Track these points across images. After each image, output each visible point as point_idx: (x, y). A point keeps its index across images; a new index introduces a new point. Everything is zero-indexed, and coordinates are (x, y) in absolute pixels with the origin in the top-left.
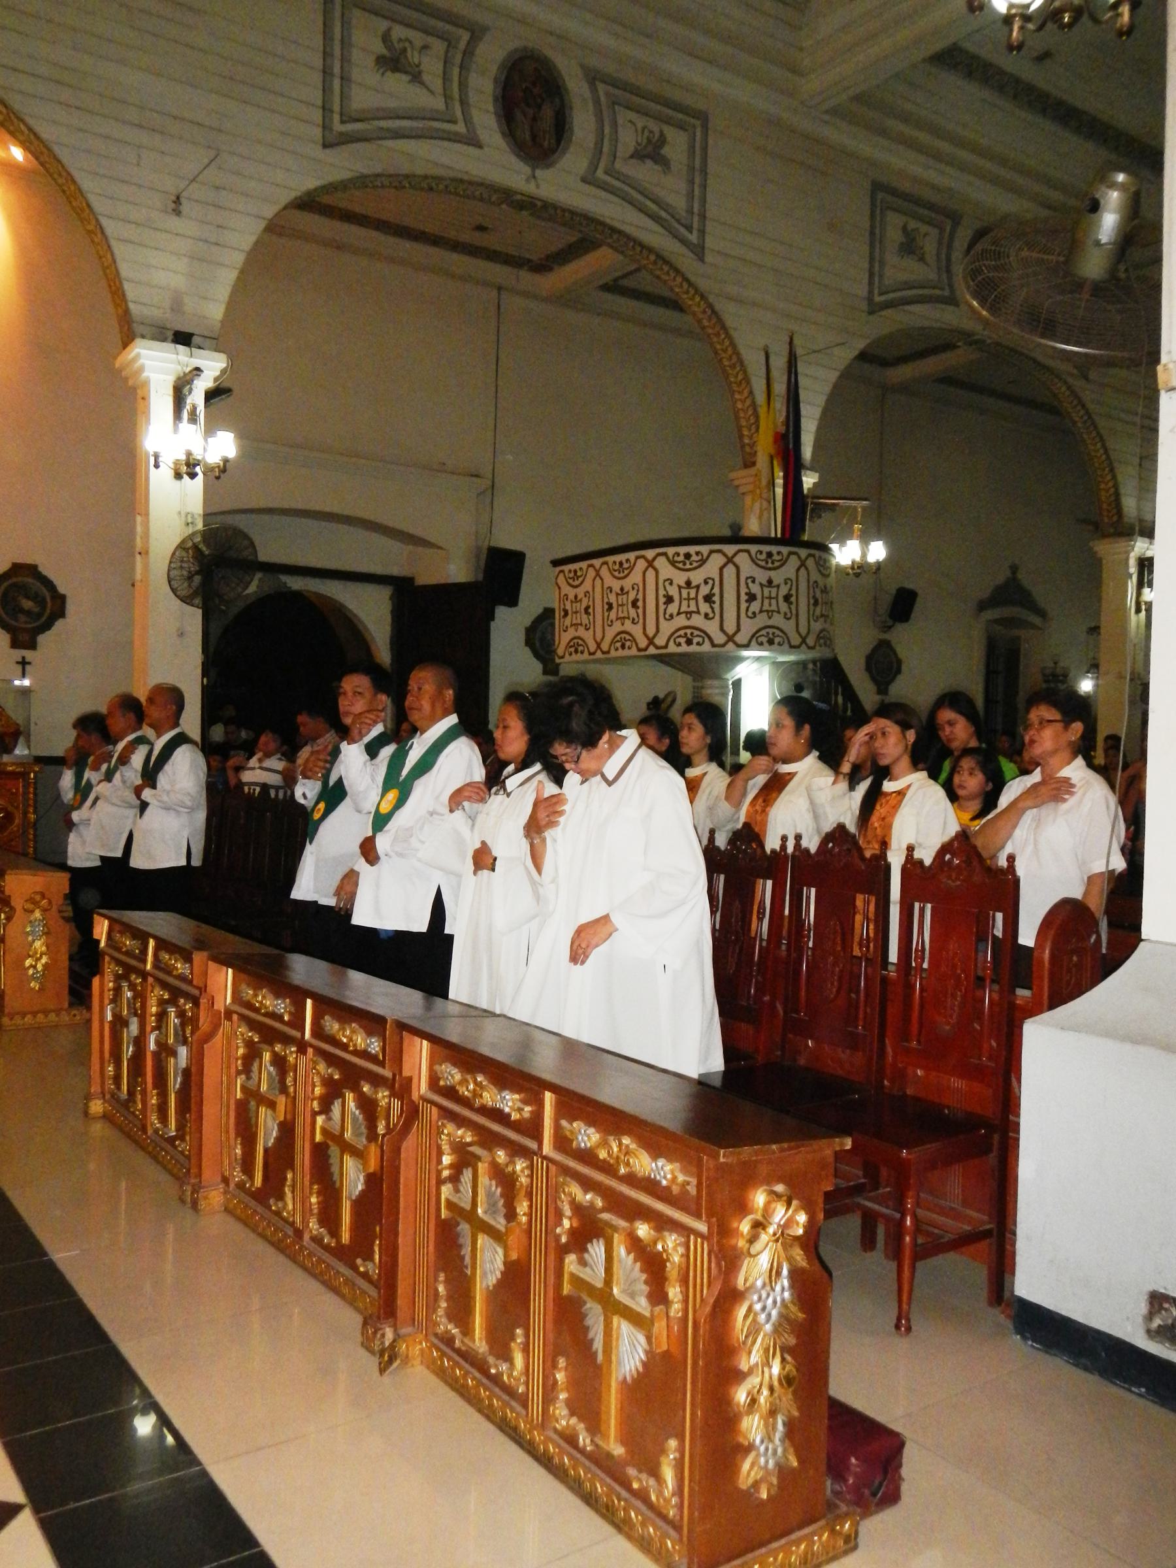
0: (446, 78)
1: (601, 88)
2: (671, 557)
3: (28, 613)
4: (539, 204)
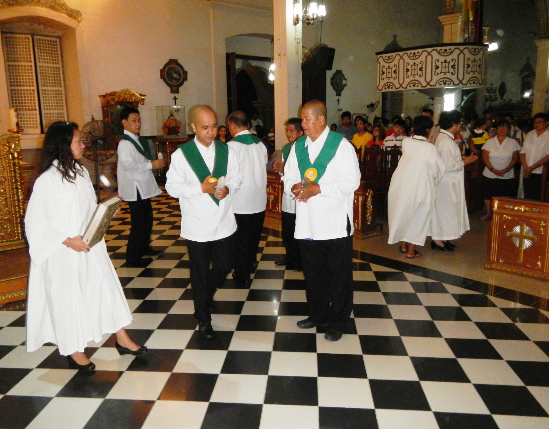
2: (439, 51)
3: (175, 79)
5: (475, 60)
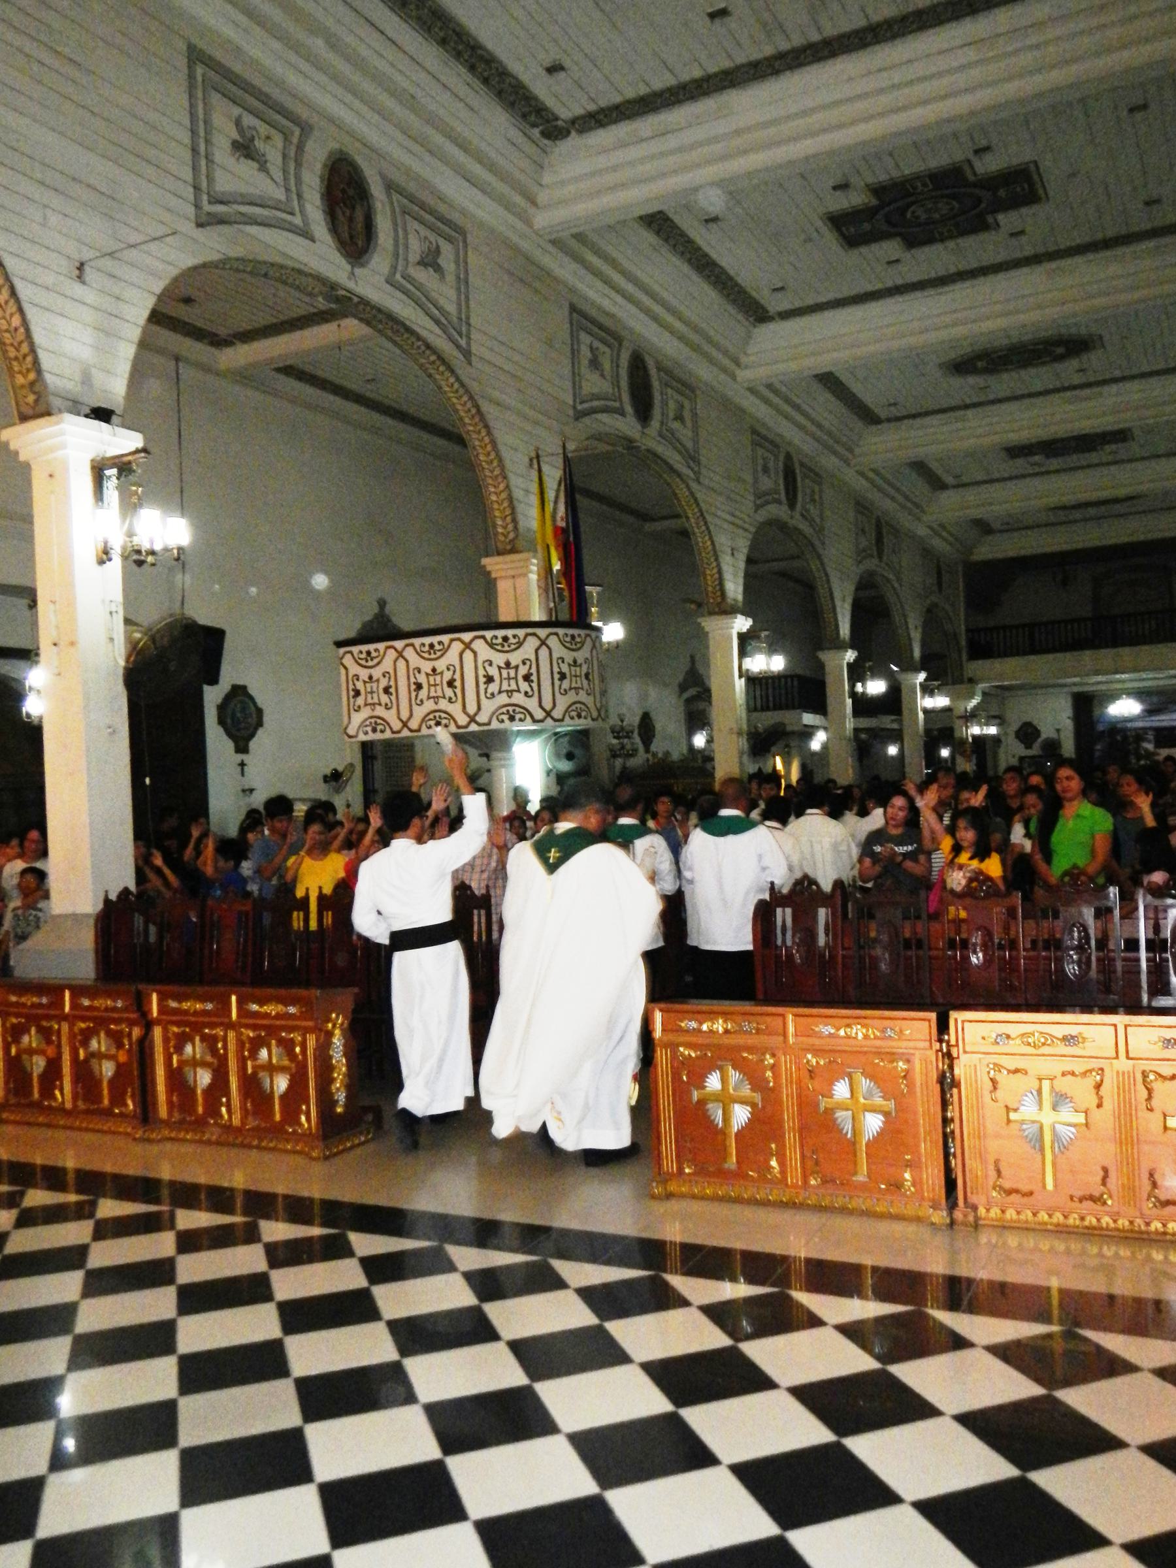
0: (285, 172)
1: (395, 196)
4: (356, 299)
5: (575, 661)
